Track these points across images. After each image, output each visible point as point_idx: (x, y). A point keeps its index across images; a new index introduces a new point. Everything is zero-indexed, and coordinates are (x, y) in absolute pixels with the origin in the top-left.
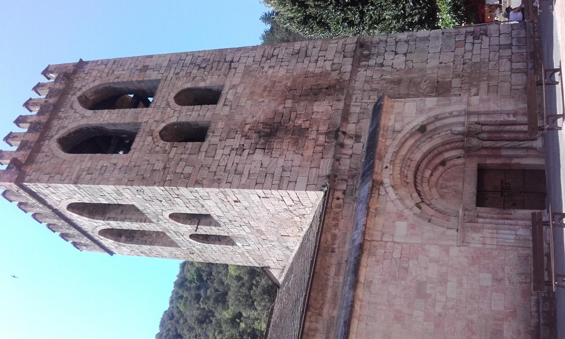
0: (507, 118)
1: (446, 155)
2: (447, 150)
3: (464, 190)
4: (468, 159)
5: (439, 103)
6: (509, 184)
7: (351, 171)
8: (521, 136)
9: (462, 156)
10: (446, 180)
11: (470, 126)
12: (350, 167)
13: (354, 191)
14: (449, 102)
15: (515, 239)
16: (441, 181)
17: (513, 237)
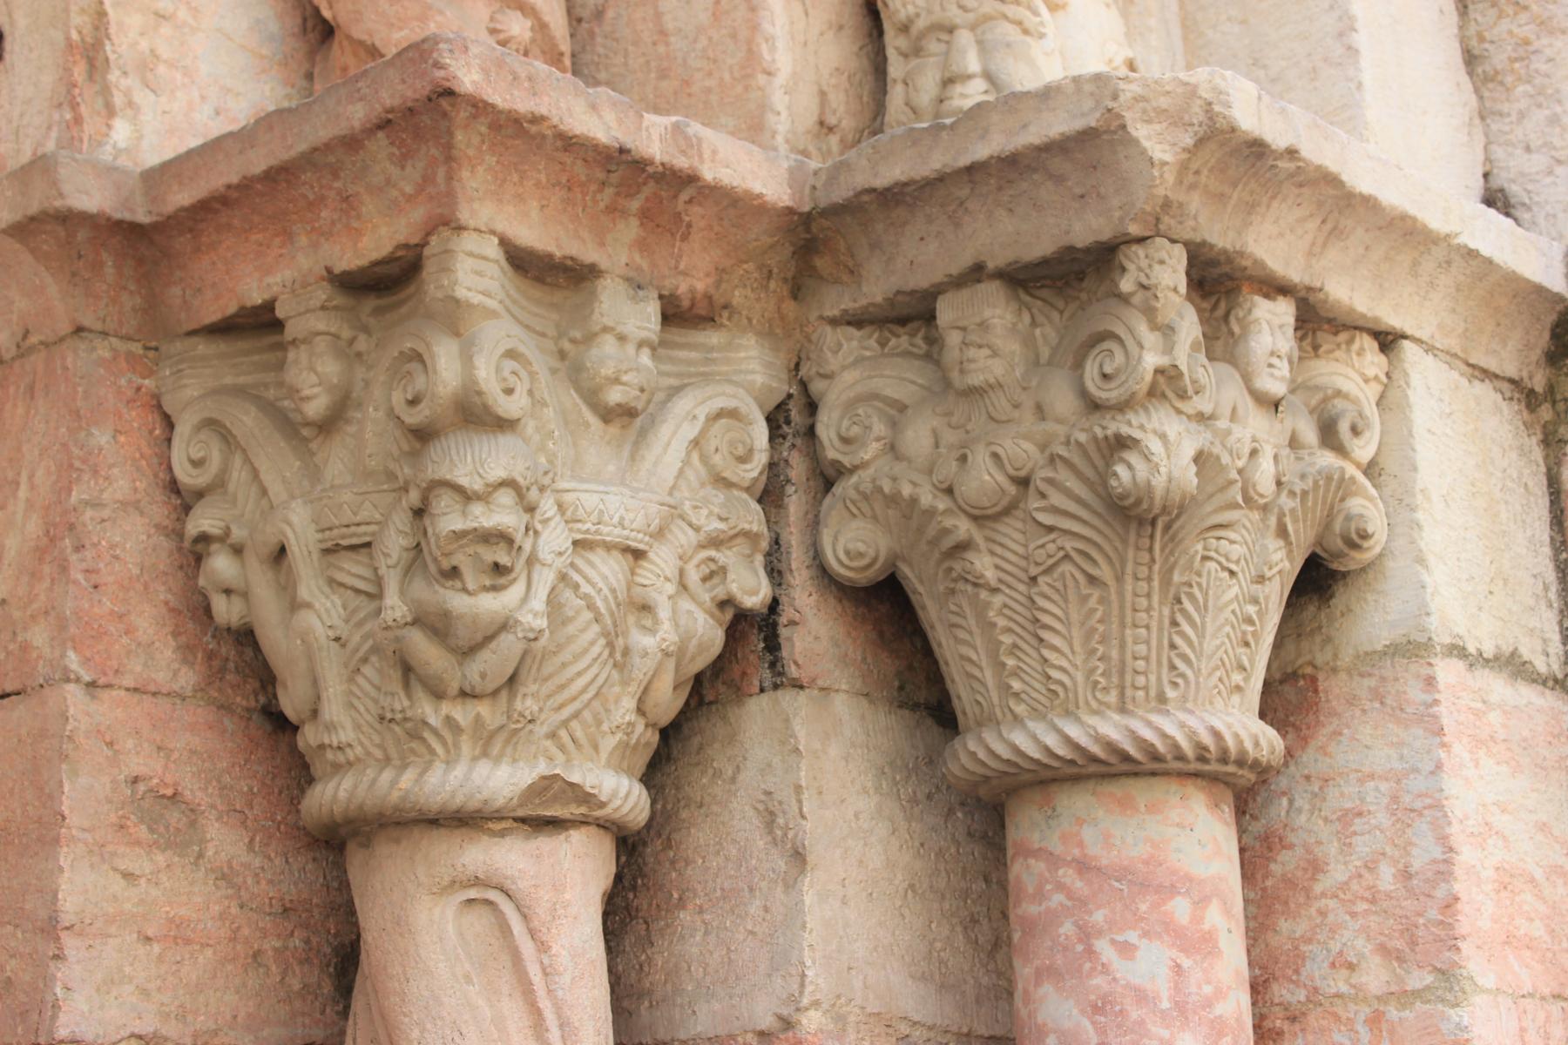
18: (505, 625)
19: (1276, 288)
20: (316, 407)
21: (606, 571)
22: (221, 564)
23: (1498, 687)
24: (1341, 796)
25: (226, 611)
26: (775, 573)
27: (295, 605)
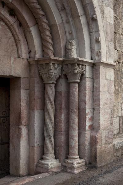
0: (88, 117)
1: (33, 31)
2: (41, 32)
9: (32, 53)
11: (81, 66)
18: (52, 77)
19: (81, 64)
20: (45, 68)
21: (55, 75)
22: (41, 73)
23: (89, 79)
24: (83, 83)
25: (41, 75)
27: (43, 75)
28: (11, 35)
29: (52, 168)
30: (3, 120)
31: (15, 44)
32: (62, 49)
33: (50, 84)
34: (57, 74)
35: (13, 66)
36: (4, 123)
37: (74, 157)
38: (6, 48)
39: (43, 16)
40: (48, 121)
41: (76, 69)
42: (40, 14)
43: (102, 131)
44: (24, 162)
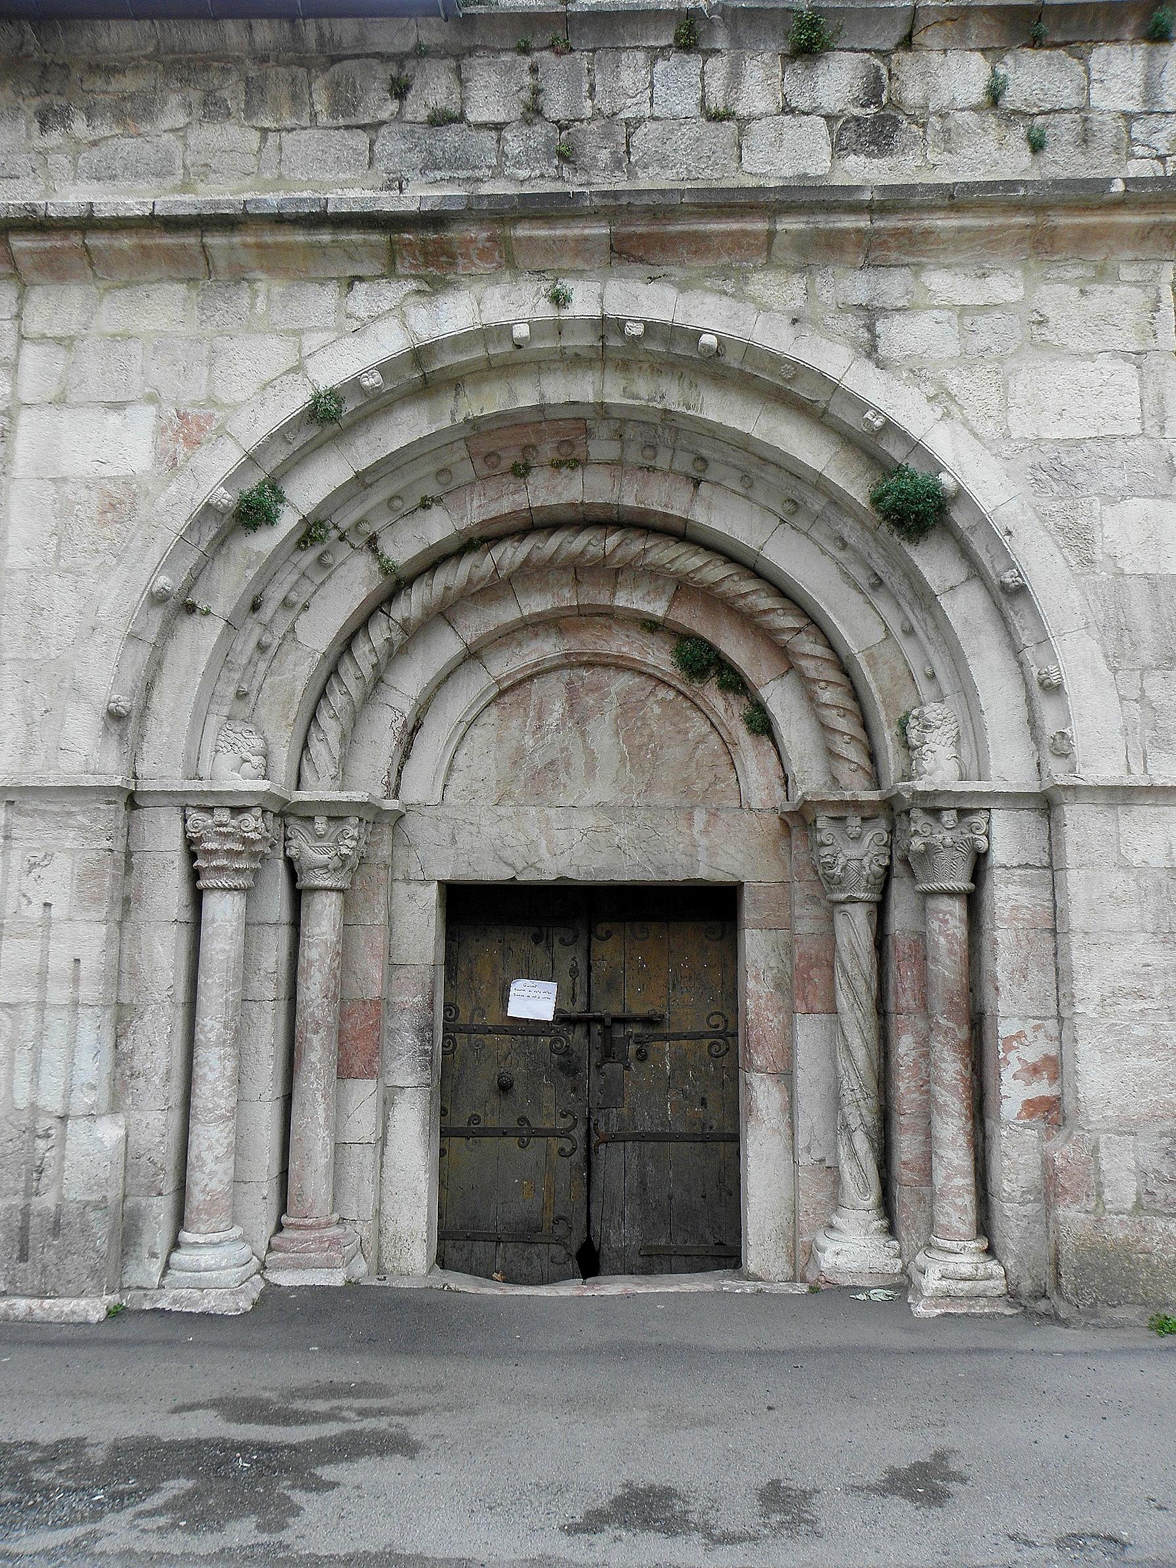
3: (552, 812)
4: (774, 820)
5: (1137, 592)
6: (642, 1057)
7: (608, 135)
8: (906, 1147)
10: (629, 708)
11: (949, 818)
12: (640, 121)
13: (463, 174)
14: (1147, 656)
15: (34, 1108)
16: (622, 682)
17: (52, 1101)
26: (891, 858)
28: (706, 728)
29: (836, 1269)
30: (711, 1045)
31: (725, 759)
32: (891, 751)
33: (843, 903)
34: (866, 860)
35: (704, 841)
36: (717, 1057)
37: (948, 1244)
38: (685, 780)
39: (799, 631)
40: (843, 1063)
41: (916, 832)
42: (783, 631)
43: (1103, 1138)
44: (770, 1225)
